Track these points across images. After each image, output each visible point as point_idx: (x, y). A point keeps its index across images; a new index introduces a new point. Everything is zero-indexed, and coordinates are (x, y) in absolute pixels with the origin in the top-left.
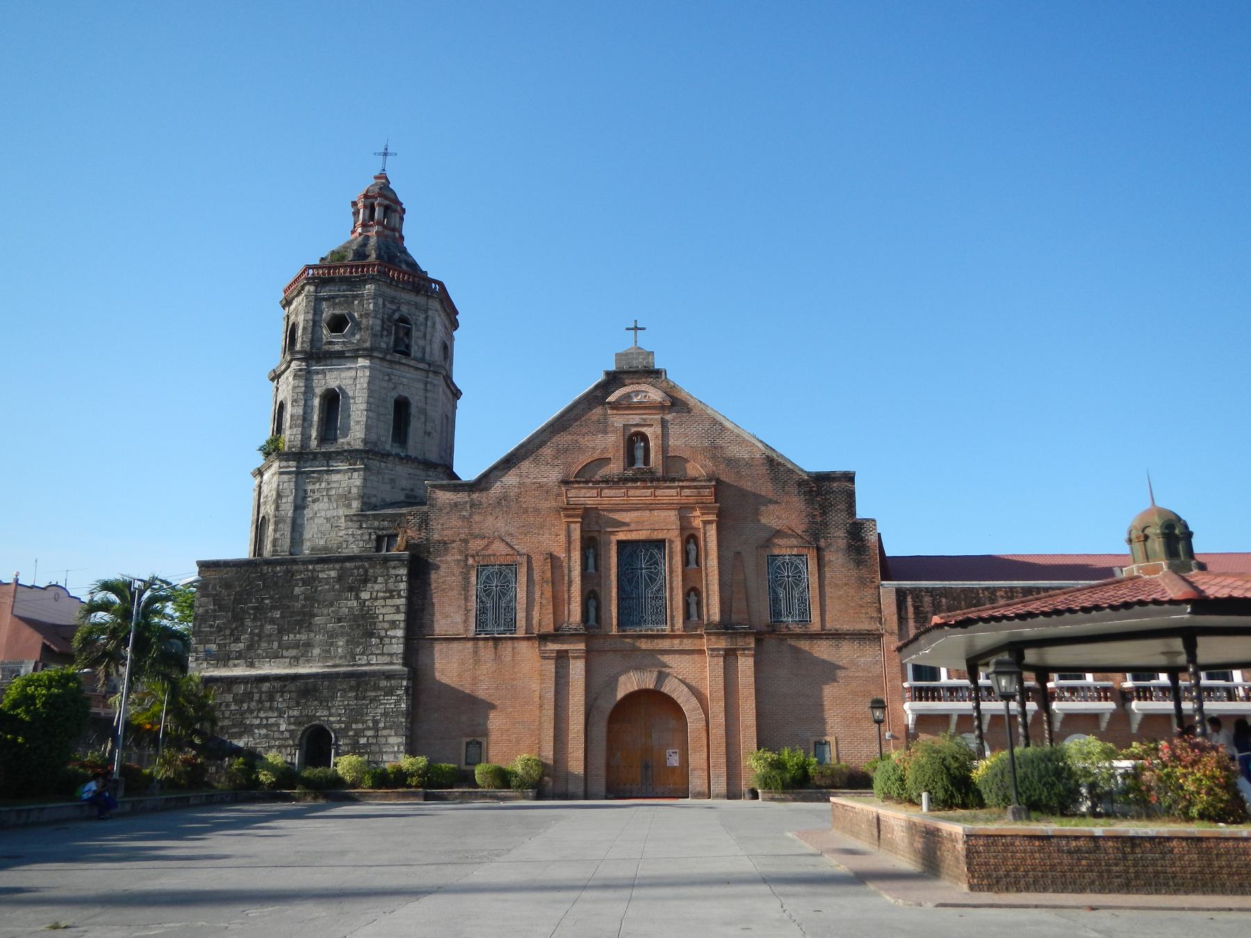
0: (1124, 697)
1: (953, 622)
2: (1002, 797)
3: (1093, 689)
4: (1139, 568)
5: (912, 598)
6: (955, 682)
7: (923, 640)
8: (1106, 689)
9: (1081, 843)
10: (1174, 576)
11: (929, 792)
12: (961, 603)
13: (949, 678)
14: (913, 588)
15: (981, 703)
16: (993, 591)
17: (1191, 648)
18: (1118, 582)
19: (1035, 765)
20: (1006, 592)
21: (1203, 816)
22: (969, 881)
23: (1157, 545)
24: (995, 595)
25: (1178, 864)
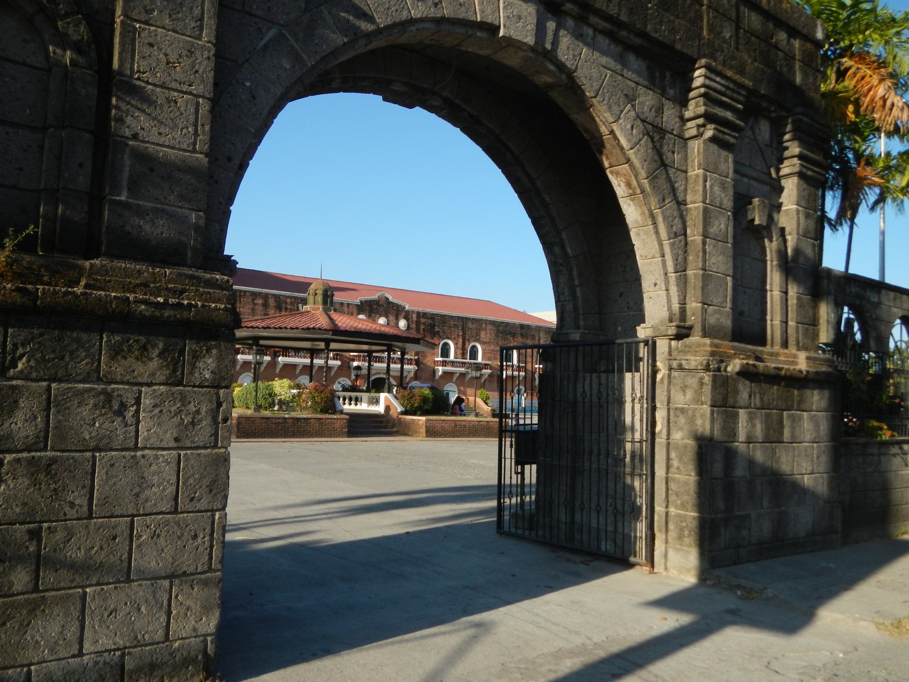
9: (280, 420)
17: (327, 346)
23: (320, 298)
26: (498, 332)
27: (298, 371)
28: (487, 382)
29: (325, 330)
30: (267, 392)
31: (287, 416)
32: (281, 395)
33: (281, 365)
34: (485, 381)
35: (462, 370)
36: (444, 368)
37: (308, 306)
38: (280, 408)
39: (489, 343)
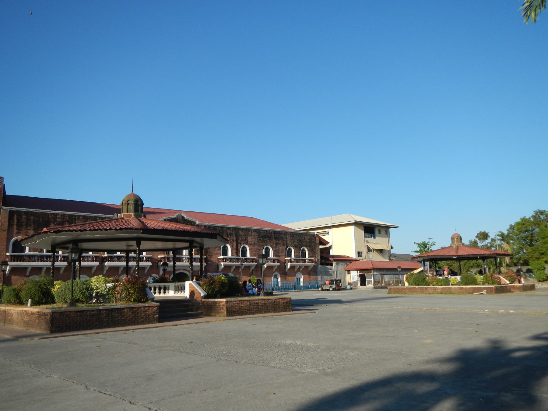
0: (103, 260)
1: (52, 231)
2: (64, 299)
3: (91, 257)
4: (124, 215)
5: (16, 215)
6: (32, 253)
7: (35, 237)
8: (96, 257)
9: (95, 312)
10: (136, 219)
11: (32, 299)
12: (40, 219)
13: (29, 251)
14: (18, 211)
15: (81, 263)
16: (57, 214)
17: (138, 245)
18: (116, 219)
19: (79, 286)
20: (61, 216)
21: (135, 300)
22: (51, 329)
23: (131, 207)
24: (56, 217)
25: (125, 316)
26: (259, 237)
27: (120, 271)
28: (254, 272)
29: (136, 229)
30: (84, 287)
31: (101, 308)
32: (97, 288)
33: (107, 268)
34: (252, 271)
35: (238, 264)
36: (225, 263)
37: (122, 214)
38: (98, 301)
39: (254, 244)
